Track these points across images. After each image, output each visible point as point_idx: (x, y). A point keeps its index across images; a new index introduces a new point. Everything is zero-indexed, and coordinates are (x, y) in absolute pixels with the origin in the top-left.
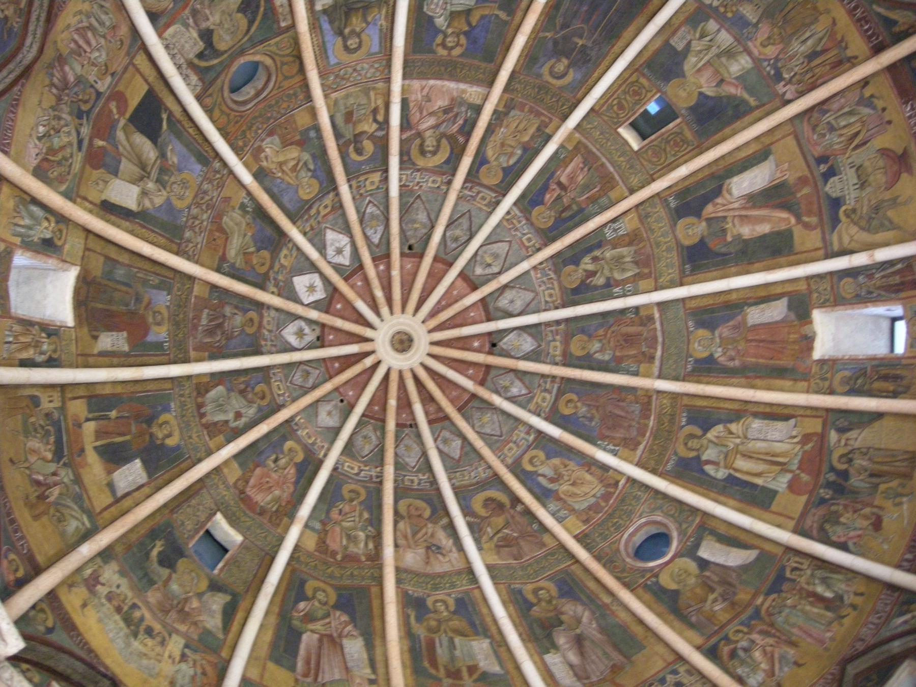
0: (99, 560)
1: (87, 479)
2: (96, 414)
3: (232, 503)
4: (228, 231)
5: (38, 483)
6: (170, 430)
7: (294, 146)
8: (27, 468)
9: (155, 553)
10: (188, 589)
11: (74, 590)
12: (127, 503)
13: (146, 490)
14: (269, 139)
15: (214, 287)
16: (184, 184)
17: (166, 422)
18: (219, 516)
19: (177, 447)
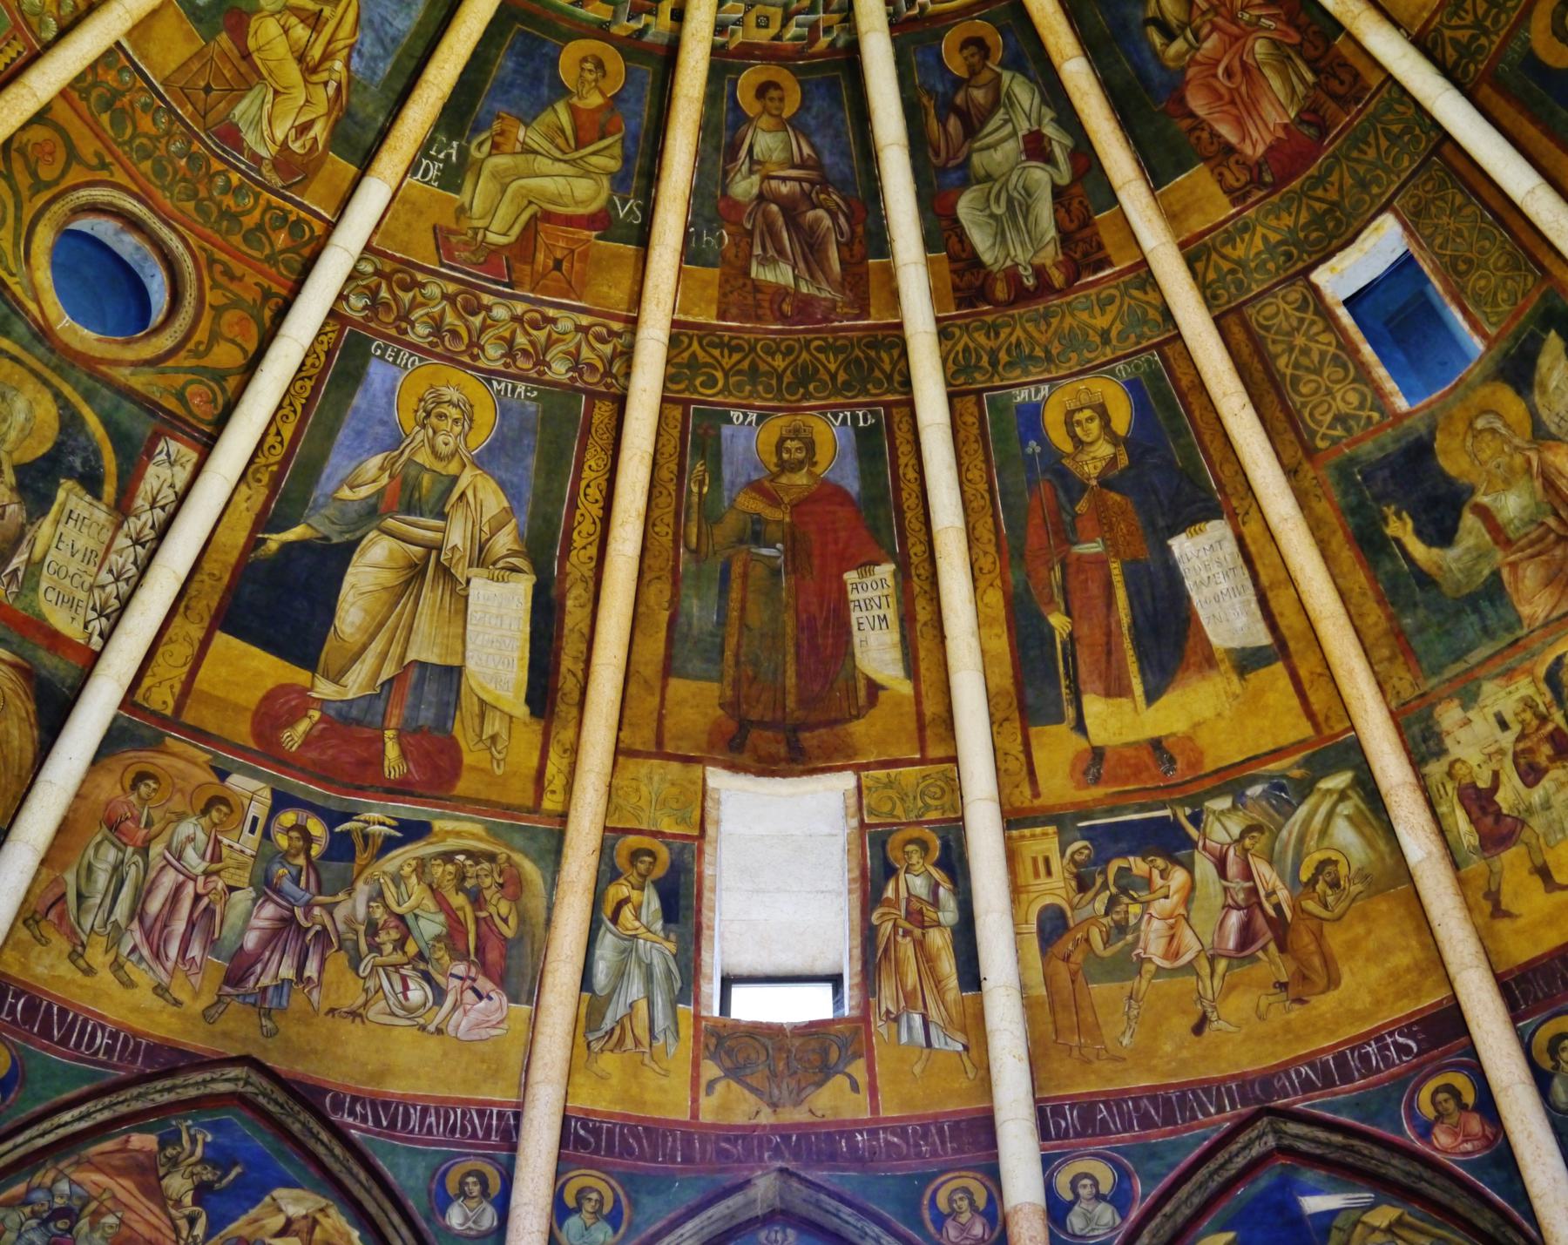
0: (1435, 769)
1: (1224, 750)
2: (1063, 683)
3: (1288, 220)
4: (525, 217)
5: (1247, 935)
6: (1086, 413)
7: (251, 44)
8: (1212, 961)
9: (1417, 549)
10: (1518, 460)
11: (1506, 902)
12: (1289, 620)
13: (1252, 529)
14: (250, 138)
15: (691, 253)
16: (430, 412)
17: (1069, 422)
18: (1320, 276)
19: (1133, 386)
